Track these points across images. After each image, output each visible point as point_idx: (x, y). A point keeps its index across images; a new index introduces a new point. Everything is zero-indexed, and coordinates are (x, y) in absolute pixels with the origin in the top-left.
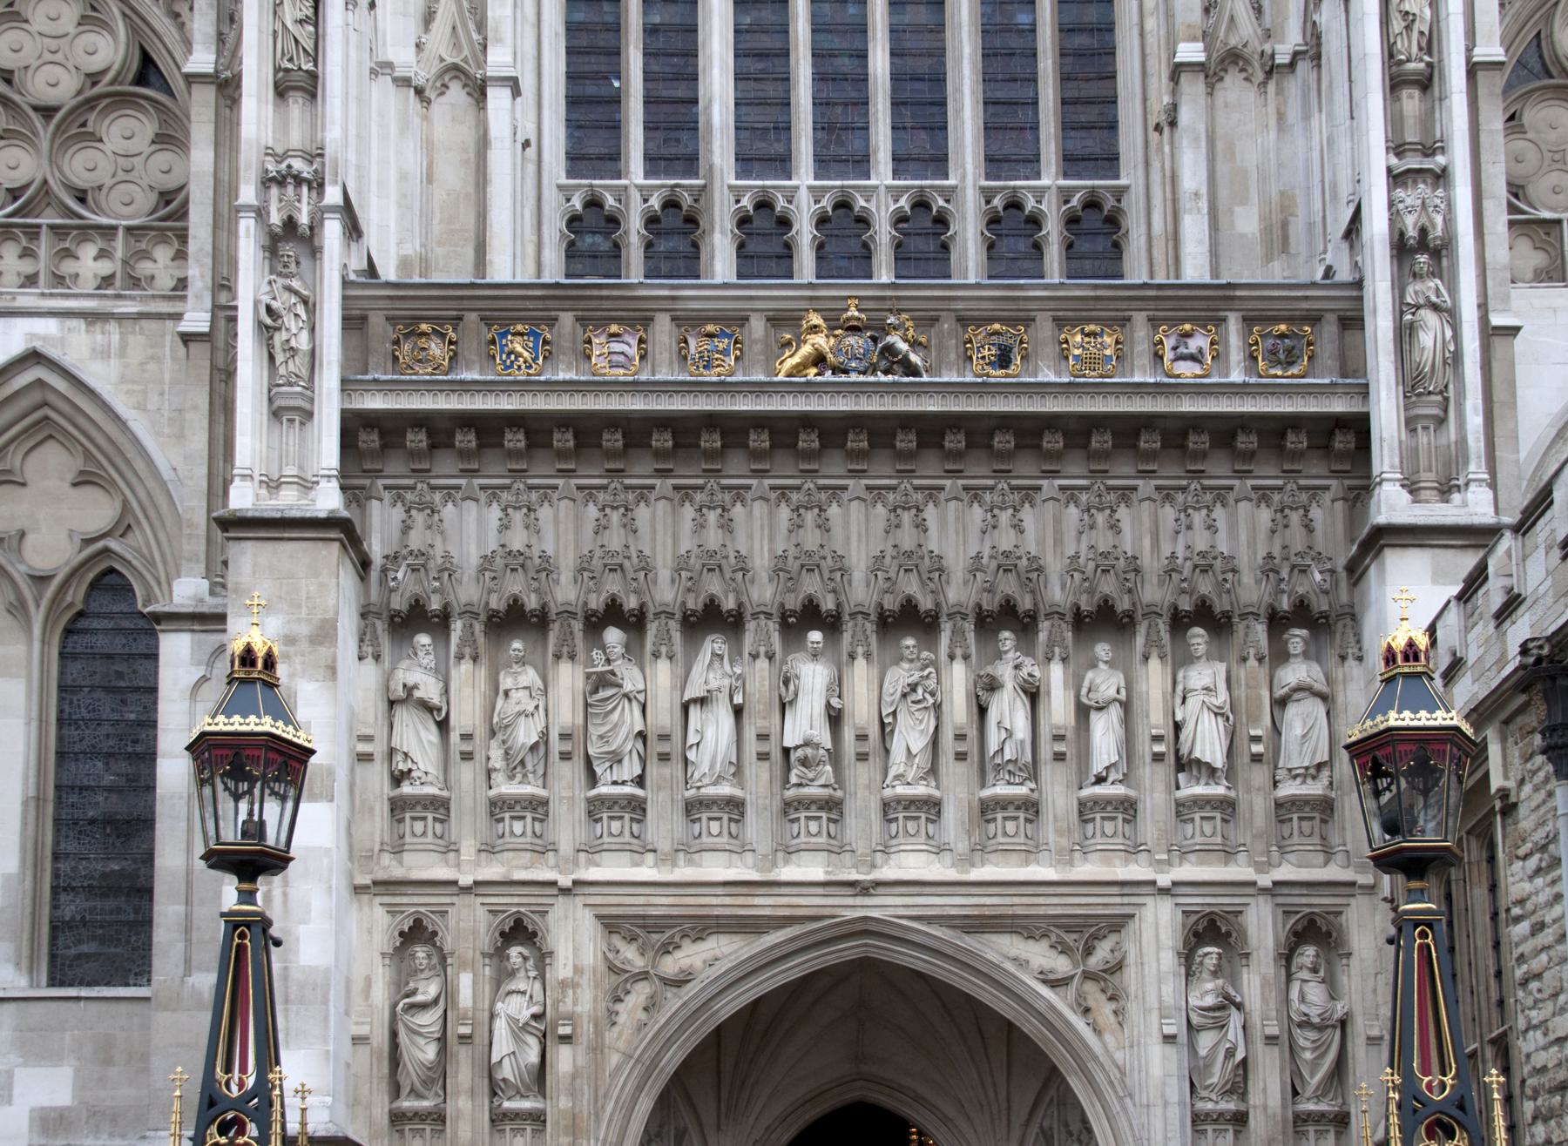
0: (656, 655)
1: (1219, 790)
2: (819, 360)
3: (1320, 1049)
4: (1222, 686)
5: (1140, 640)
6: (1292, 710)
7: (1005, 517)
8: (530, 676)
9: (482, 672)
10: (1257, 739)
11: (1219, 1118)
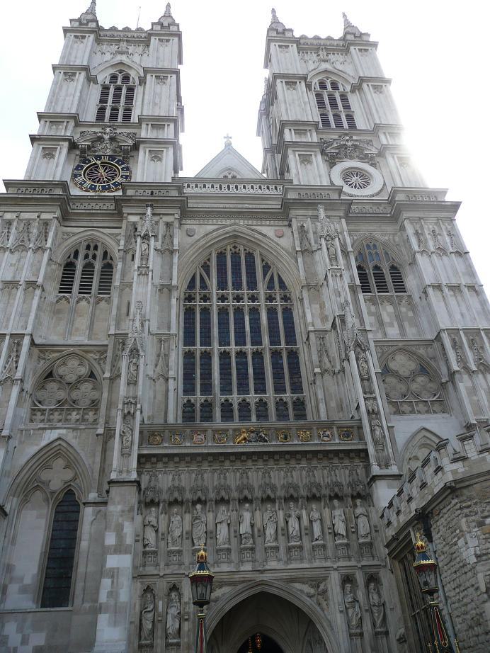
0: (209, 511)
1: (345, 541)
2: (245, 439)
3: (379, 612)
4: (343, 515)
5: (323, 503)
6: (359, 520)
7: (289, 474)
8: (179, 518)
9: (167, 516)
10: (352, 528)
11: (356, 635)
